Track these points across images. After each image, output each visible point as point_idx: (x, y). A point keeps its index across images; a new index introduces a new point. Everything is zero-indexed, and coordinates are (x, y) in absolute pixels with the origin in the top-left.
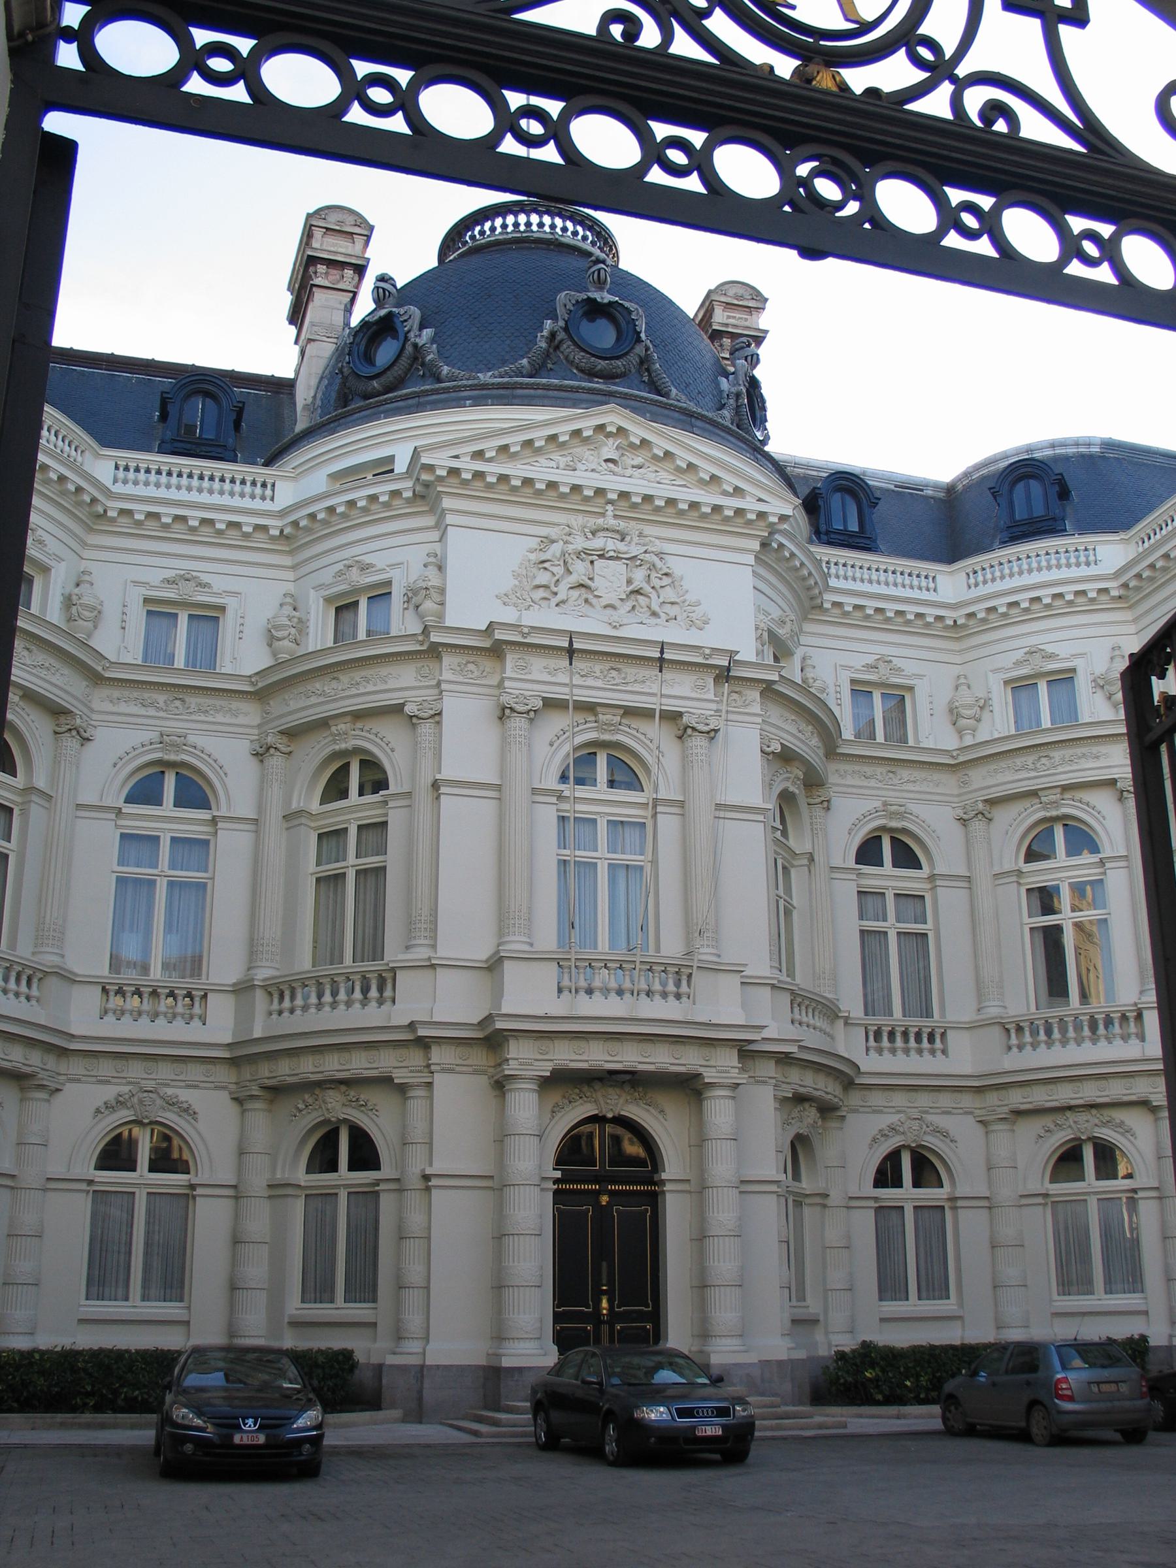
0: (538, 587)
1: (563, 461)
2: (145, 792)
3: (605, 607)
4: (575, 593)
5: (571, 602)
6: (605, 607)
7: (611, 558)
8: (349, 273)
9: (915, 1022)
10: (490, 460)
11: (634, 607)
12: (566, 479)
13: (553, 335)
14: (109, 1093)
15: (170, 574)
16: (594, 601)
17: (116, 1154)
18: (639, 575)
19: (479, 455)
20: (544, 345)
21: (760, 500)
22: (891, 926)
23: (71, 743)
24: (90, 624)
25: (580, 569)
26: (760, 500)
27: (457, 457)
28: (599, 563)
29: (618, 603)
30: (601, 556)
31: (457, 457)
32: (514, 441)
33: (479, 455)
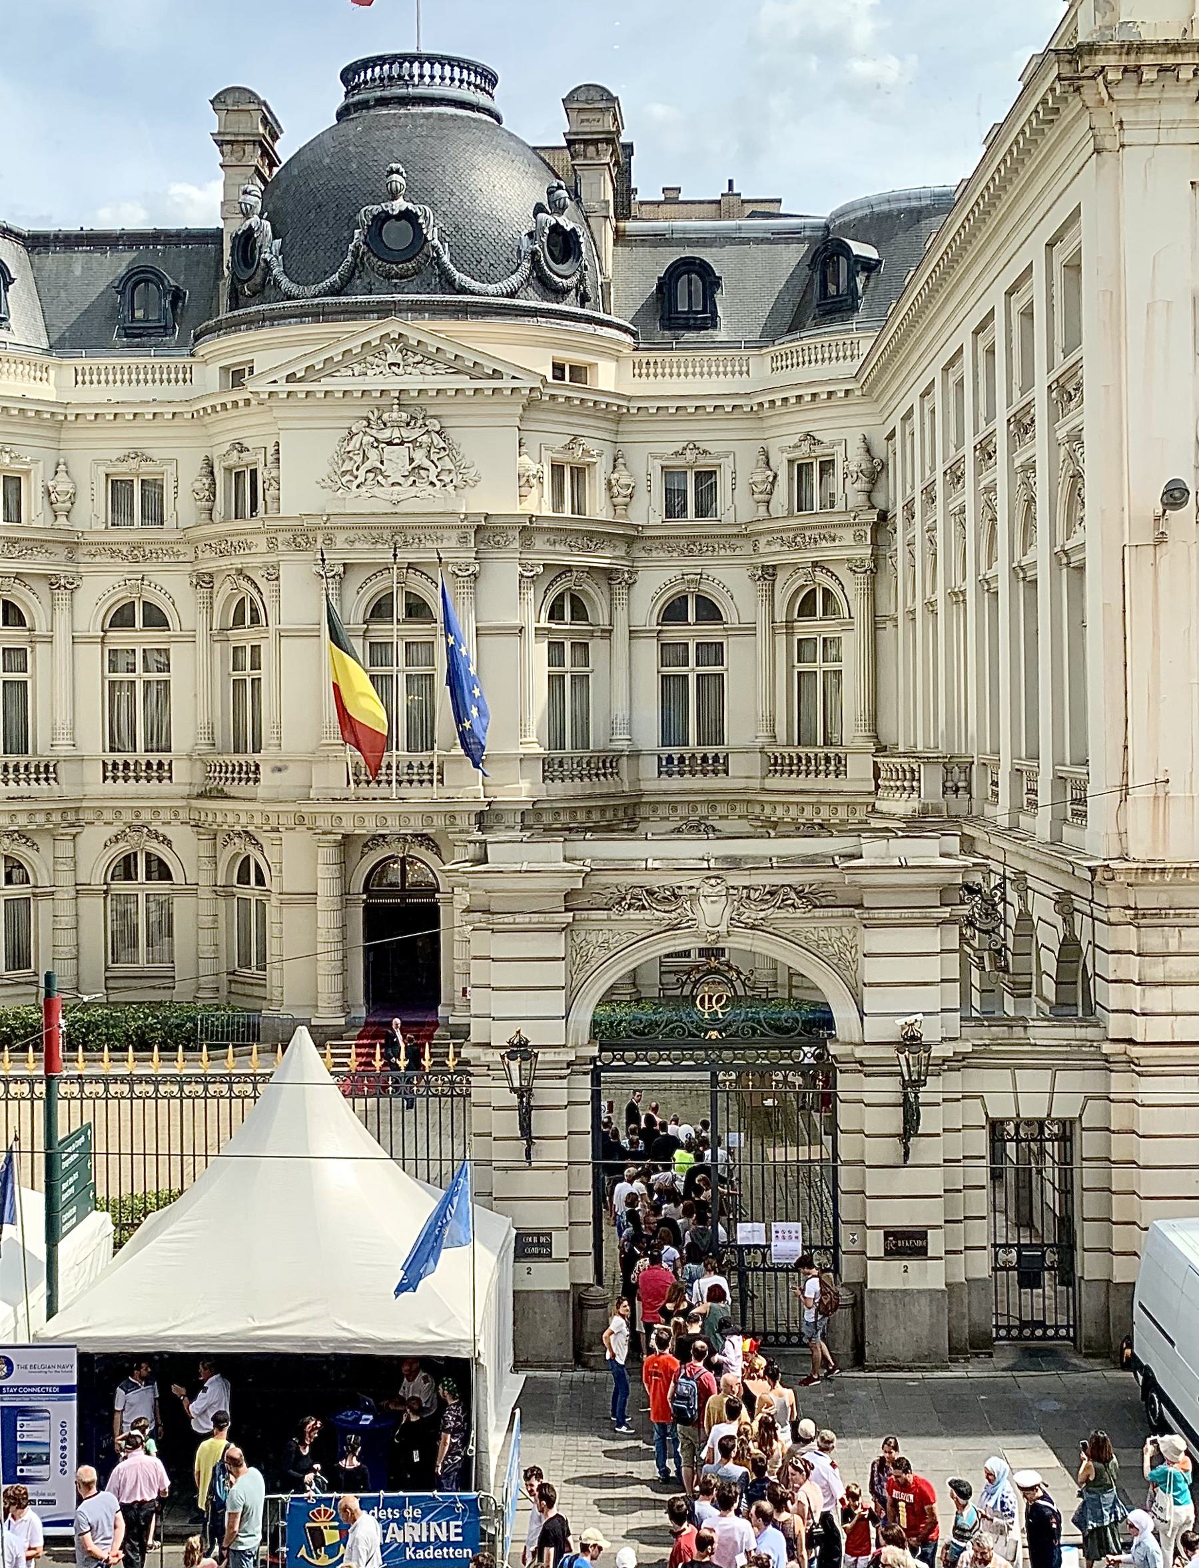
0: (344, 473)
1: (358, 369)
2: (122, 618)
3: (393, 484)
4: (371, 475)
5: (368, 482)
6: (393, 484)
7: (397, 444)
8: (249, 148)
9: (700, 751)
10: (300, 380)
11: (414, 482)
12: (357, 385)
13: (357, 248)
14: (112, 831)
15: (121, 454)
16: (383, 482)
17: (126, 868)
18: (420, 456)
19: (290, 378)
20: (349, 258)
21: (514, 378)
22: (692, 671)
23: (63, 594)
24: (68, 504)
25: (373, 454)
26: (514, 378)
27: (275, 382)
28: (388, 449)
29: (401, 480)
30: (390, 444)
31: (275, 382)
32: (317, 361)
33: (290, 378)
